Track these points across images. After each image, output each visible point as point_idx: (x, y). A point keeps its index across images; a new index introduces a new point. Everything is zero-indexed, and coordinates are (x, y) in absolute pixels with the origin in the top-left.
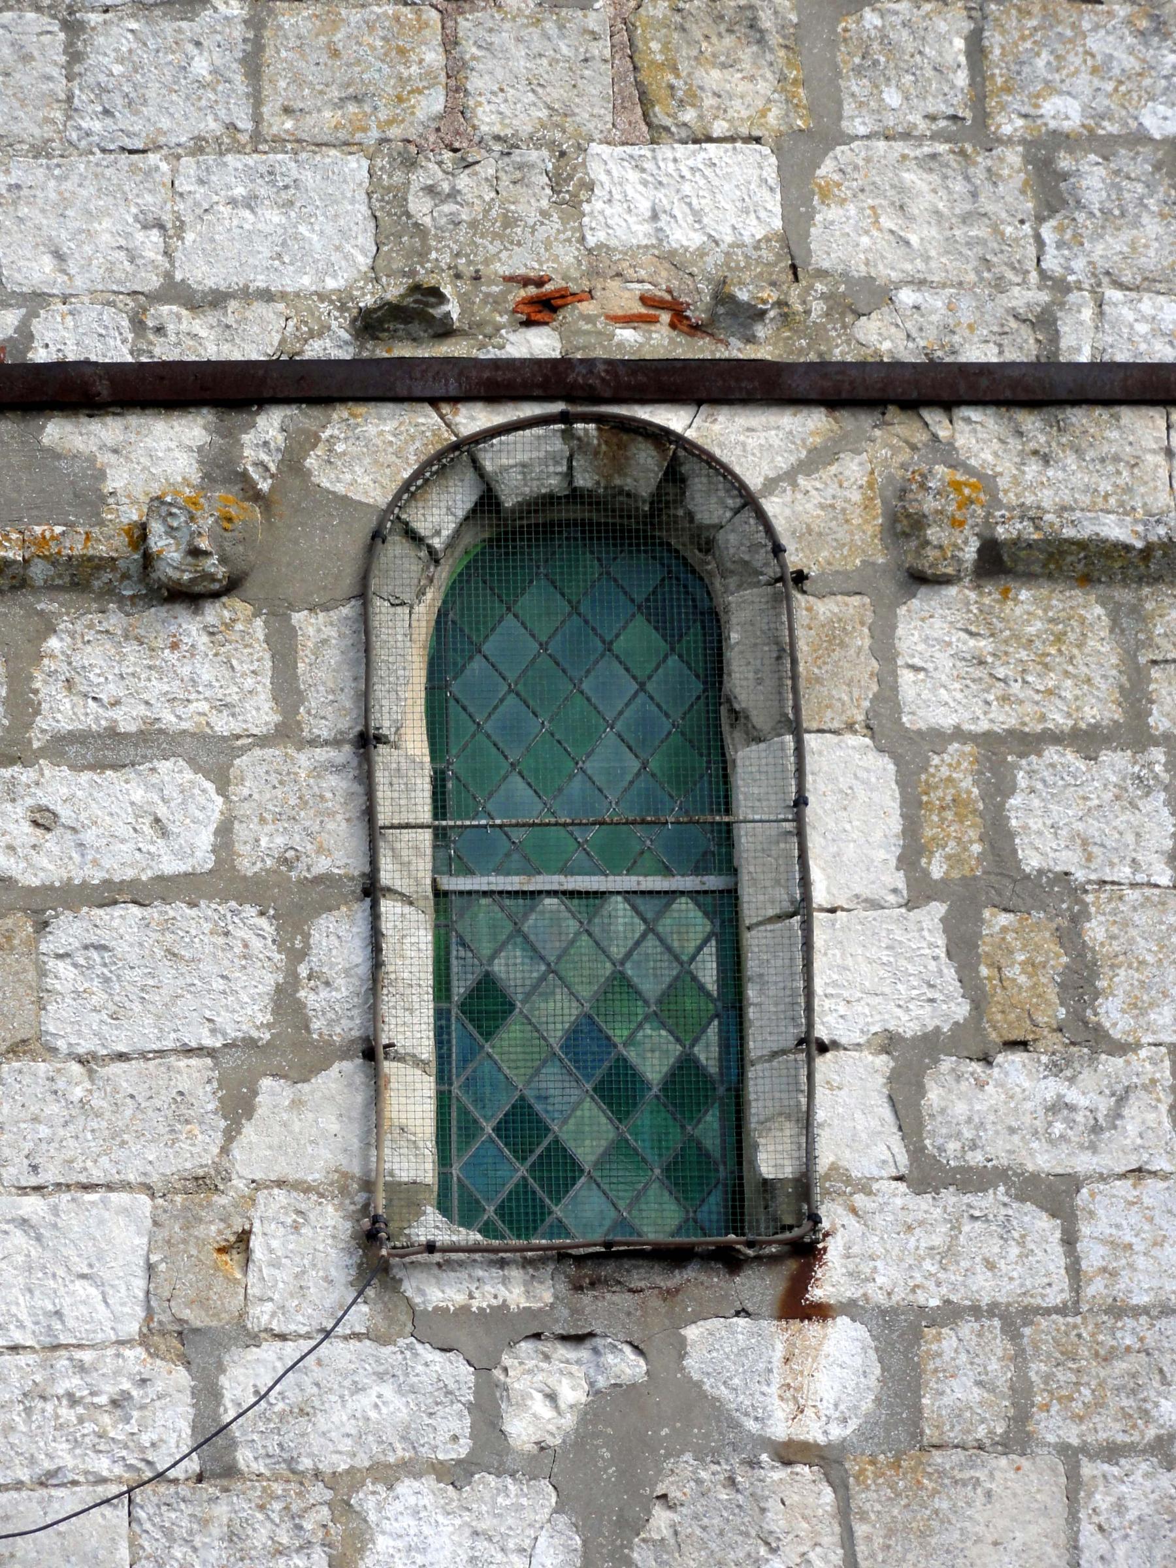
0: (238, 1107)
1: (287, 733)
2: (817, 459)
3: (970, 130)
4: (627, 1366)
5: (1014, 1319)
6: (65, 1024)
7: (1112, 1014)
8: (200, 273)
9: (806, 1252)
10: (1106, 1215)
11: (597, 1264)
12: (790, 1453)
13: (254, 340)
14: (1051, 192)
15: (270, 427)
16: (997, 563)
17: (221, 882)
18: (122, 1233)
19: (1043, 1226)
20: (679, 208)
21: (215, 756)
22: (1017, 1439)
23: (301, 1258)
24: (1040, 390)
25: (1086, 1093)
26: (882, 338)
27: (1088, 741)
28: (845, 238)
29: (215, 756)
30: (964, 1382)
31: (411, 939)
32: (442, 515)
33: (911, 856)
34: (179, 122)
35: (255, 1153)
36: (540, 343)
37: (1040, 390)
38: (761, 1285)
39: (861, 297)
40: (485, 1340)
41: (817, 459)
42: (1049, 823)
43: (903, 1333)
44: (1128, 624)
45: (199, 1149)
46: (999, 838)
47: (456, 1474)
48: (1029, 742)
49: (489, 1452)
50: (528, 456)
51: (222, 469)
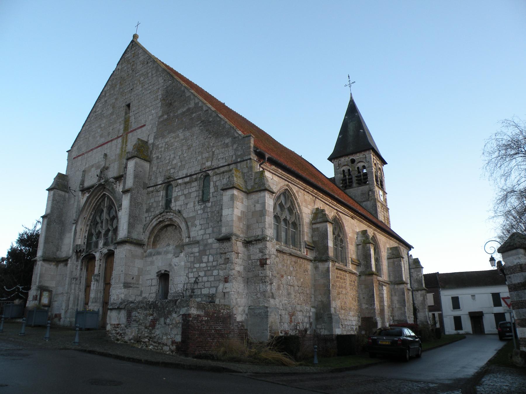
16: (216, 175)
20: (208, 164)
21: (195, 187)
23: (196, 203)
24: (218, 168)
29: (195, 187)
30: (213, 204)
32: (202, 177)
37: (218, 168)
43: (212, 202)
50: (204, 174)
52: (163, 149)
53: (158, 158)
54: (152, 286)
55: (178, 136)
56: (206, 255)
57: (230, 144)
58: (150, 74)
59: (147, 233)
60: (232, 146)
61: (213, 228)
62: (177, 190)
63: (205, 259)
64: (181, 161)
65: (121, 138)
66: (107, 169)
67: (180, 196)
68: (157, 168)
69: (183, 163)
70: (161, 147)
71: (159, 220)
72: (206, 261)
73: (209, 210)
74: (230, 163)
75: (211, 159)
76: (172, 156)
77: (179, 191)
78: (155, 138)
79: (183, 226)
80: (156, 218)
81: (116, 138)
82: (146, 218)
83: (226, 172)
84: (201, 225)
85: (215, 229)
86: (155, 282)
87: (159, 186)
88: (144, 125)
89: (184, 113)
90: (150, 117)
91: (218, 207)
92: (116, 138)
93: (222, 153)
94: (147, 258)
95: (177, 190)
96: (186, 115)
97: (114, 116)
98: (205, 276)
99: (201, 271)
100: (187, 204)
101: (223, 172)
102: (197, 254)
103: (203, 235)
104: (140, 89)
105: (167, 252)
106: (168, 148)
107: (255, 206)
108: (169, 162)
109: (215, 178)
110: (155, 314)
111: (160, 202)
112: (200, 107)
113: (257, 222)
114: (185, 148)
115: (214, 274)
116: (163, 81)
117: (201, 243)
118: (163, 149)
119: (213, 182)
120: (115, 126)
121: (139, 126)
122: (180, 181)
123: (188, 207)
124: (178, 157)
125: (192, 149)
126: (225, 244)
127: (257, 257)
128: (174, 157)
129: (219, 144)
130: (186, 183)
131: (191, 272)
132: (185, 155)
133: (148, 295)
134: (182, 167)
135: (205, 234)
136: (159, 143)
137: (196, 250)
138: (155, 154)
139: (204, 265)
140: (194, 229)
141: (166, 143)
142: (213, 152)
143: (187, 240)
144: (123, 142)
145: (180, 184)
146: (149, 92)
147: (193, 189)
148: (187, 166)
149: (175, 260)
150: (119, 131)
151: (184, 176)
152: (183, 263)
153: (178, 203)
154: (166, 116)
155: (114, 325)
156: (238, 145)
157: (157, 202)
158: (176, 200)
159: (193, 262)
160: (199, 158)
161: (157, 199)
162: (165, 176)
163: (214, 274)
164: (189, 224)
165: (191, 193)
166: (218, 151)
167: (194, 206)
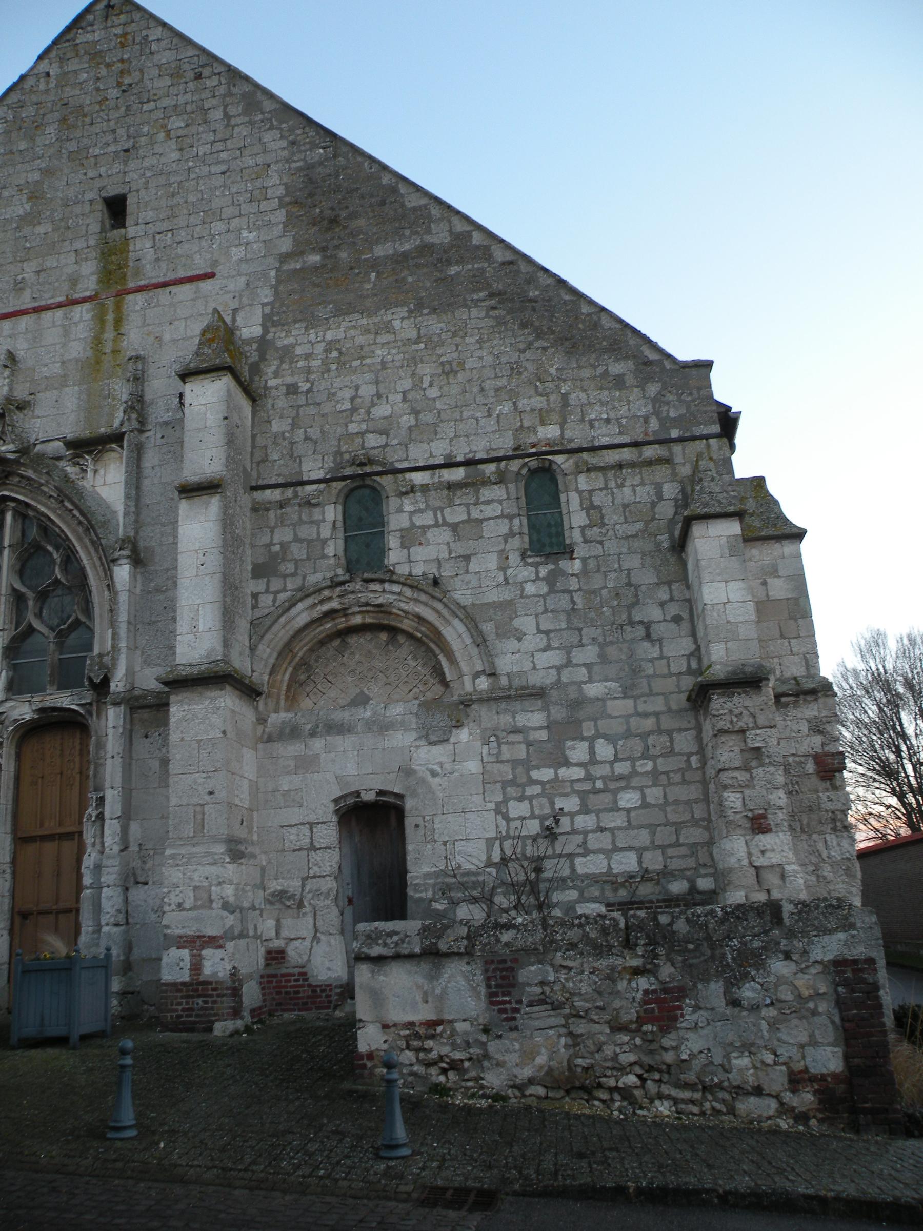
0: (506, 542)
1: (508, 498)
2: (567, 460)
3: (582, 420)
4: (553, 567)
5: (597, 557)
6: (486, 534)
7: (606, 521)
8: (494, 447)
9: (572, 552)
10: (607, 544)
11: (548, 556)
12: (572, 575)
13: (501, 454)
14: (592, 426)
15: (504, 463)
17: (502, 516)
18: (494, 557)
19: (599, 546)
21: (500, 502)
22: (598, 571)
24: (593, 449)
25: (604, 531)
26: (573, 445)
27: (601, 490)
28: (568, 434)
30: (592, 564)
31: (525, 521)
32: (524, 471)
33: (581, 505)
34: (490, 429)
35: (508, 547)
36: (534, 450)
37: (593, 449)
38: (567, 556)
39: (571, 441)
40: (536, 565)
41: (567, 460)
42: (597, 500)
43: (584, 560)
44: (605, 476)
45: (501, 547)
46: (591, 502)
47: (534, 581)
48: (594, 490)
49: (538, 578)
50: (534, 463)
51: (498, 468)
52: (316, 363)
53: (292, 389)
54: (312, 848)
55: (388, 328)
56: (583, 739)
57: (630, 380)
58: (218, 114)
59: (267, 652)
60: (642, 386)
61: (602, 646)
62: (408, 508)
63: (578, 751)
64: (416, 413)
65: (87, 306)
66: (20, 408)
67: (425, 528)
68: (294, 425)
69: (427, 418)
70: (308, 356)
71: (326, 607)
72: (585, 757)
73: (574, 584)
74: (640, 438)
75: (556, 417)
76: (367, 391)
77: (420, 511)
78: (268, 322)
79: (455, 634)
80: (309, 601)
81: (60, 305)
82: (255, 596)
83: (633, 465)
84: (547, 633)
85: (611, 651)
86: (329, 834)
87: (309, 488)
88: (212, 275)
89: (405, 256)
90: (237, 253)
91: (613, 575)
92: (60, 305)
93: (603, 404)
94: (276, 745)
95: (408, 508)
96: (417, 266)
97: (41, 229)
98: (585, 810)
99: (566, 795)
100: (467, 558)
101: (620, 466)
102: (543, 735)
103: (559, 669)
104: (175, 155)
105: (383, 727)
106: (341, 364)
107: (764, 583)
108: (354, 410)
109: (583, 482)
110: (666, 971)
111: (324, 542)
112: (477, 247)
113: (782, 636)
114: (426, 370)
115: (622, 804)
116: (284, 143)
117: (554, 693)
118: (316, 363)
119: (580, 493)
120: (51, 262)
121: (181, 274)
122: (419, 478)
123: (474, 566)
124: (399, 397)
125: (461, 377)
126: (736, 699)
127: (804, 748)
128: (379, 396)
129: (586, 373)
130: (451, 487)
131: (521, 799)
132: (433, 393)
133: (297, 883)
134: (423, 431)
135: (569, 664)
136: (291, 340)
137: (533, 718)
138: (276, 375)
139: (577, 773)
140: (512, 644)
141: (330, 346)
142: (565, 397)
143: (483, 683)
144: (100, 319)
145: (425, 488)
146: (223, 168)
147: (493, 510)
148: (448, 430)
149: (429, 756)
150: (74, 281)
151: (441, 461)
152: (473, 766)
153: (419, 553)
154: (315, 258)
155: (411, 1024)
156: (664, 388)
157: (310, 542)
158: (410, 538)
159: (527, 765)
160: (506, 408)
161: (306, 532)
162: (339, 453)
163: (622, 804)
164: (488, 628)
165: (480, 521)
166: (583, 395)
167: (503, 569)
